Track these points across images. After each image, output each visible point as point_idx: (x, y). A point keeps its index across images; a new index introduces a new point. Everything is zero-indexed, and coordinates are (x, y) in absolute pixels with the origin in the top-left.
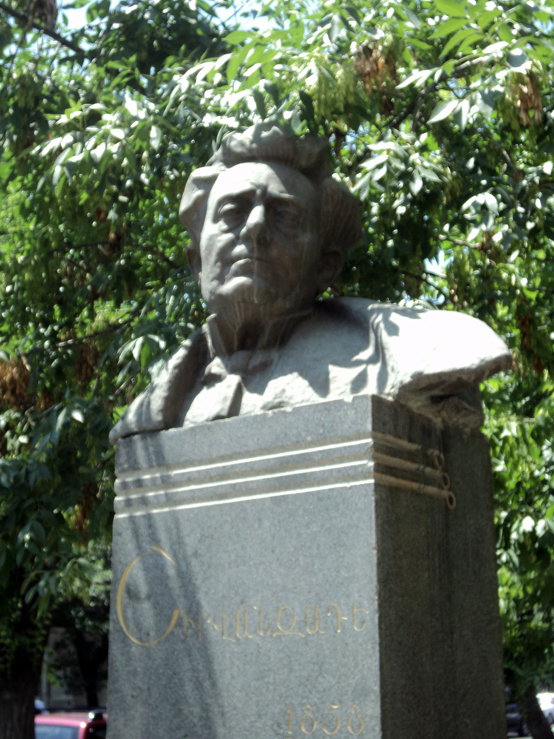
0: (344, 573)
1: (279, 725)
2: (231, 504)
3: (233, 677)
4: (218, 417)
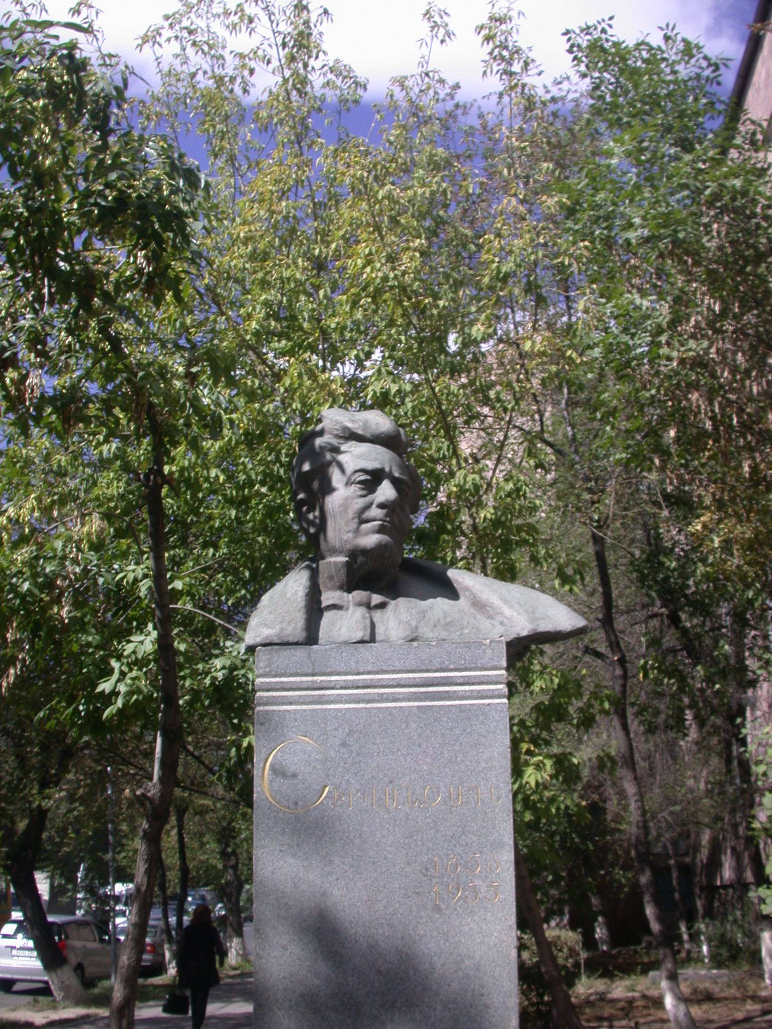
0: (483, 764)
1: (427, 869)
2: (379, 709)
3: (383, 836)
4: (362, 642)
